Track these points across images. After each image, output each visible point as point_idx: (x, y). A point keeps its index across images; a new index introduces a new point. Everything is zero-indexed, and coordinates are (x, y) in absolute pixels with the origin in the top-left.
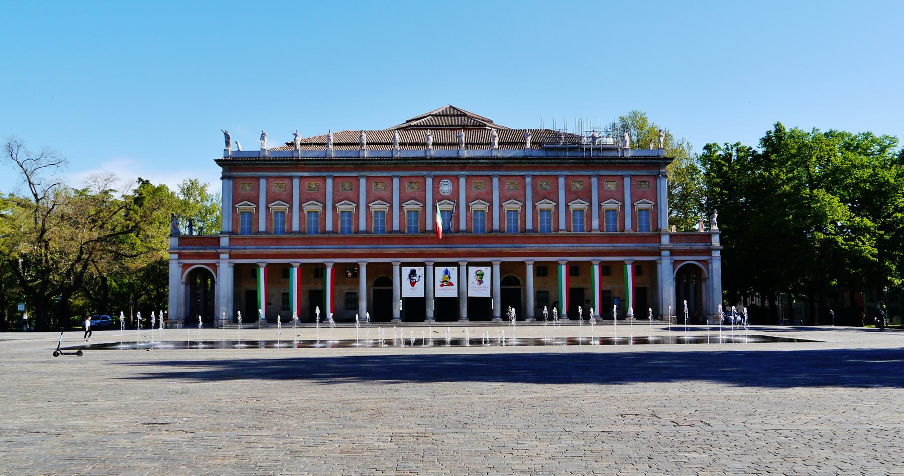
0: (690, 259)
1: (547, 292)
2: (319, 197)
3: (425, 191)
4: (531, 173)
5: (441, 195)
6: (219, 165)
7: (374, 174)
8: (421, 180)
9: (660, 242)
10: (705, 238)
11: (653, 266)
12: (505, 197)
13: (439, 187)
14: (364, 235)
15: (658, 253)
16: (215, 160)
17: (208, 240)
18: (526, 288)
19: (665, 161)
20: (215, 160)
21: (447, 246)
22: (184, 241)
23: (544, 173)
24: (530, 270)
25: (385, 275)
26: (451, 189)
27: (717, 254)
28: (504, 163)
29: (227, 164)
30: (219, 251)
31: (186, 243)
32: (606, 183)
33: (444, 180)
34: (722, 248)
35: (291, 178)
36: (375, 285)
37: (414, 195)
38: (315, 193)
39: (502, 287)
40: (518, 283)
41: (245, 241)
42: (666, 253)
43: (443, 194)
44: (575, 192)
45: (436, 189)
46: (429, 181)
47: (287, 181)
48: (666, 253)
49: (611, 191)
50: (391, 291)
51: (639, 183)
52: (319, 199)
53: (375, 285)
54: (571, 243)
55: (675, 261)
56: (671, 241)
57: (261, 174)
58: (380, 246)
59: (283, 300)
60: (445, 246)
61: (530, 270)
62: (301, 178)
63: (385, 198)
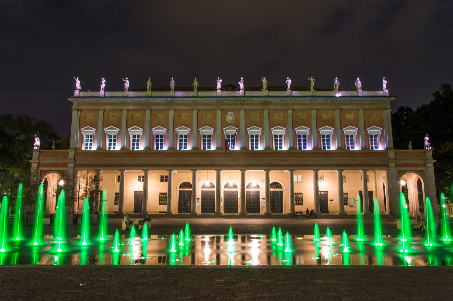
1: (302, 194)
3: (216, 120)
5: (227, 123)
7: (179, 108)
13: (226, 117)
14: (171, 150)
21: (232, 159)
22: (43, 154)
30: (67, 161)
31: (45, 155)
33: (230, 112)
35: (121, 110)
43: (228, 122)
46: (219, 112)
57: (100, 107)
58: (183, 159)
59: (115, 198)
60: (230, 159)
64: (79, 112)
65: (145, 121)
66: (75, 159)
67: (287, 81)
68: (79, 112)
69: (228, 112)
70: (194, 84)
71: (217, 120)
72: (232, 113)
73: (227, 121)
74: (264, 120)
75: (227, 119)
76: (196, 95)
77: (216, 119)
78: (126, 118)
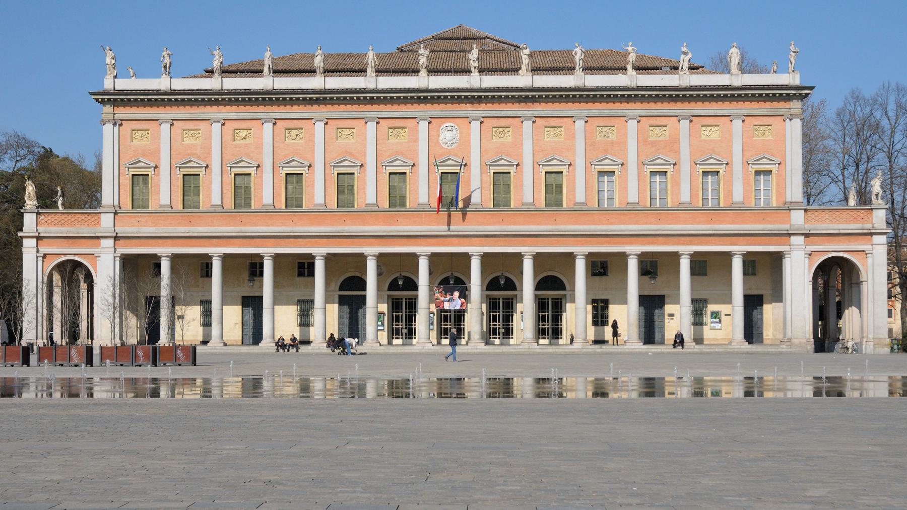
0: (836, 249)
3: (416, 140)
6: (97, 100)
9: (789, 221)
10: (862, 215)
11: (776, 259)
12: (543, 151)
13: (439, 136)
16: (92, 94)
17: (83, 217)
18: (574, 294)
19: (800, 92)
20: (92, 94)
22: (46, 219)
24: (580, 266)
25: (357, 274)
26: (458, 137)
28: (541, 96)
29: (109, 100)
32: (704, 128)
36: (341, 289)
38: (246, 145)
39: (540, 293)
40: (564, 289)
41: (139, 219)
43: (445, 146)
44: (653, 144)
45: (432, 140)
46: (423, 125)
47: (202, 125)
49: (711, 141)
50: (364, 298)
51: (756, 128)
52: (252, 155)
53: (341, 289)
54: (646, 223)
55: (812, 251)
56: (806, 220)
61: (580, 266)
64: (116, 128)
66: (115, 231)
67: (574, 52)
68: (116, 128)
69: (444, 122)
70: (368, 59)
71: (419, 142)
72: (452, 127)
73: (442, 144)
74: (524, 141)
75: (441, 138)
76: (372, 86)
77: (418, 138)
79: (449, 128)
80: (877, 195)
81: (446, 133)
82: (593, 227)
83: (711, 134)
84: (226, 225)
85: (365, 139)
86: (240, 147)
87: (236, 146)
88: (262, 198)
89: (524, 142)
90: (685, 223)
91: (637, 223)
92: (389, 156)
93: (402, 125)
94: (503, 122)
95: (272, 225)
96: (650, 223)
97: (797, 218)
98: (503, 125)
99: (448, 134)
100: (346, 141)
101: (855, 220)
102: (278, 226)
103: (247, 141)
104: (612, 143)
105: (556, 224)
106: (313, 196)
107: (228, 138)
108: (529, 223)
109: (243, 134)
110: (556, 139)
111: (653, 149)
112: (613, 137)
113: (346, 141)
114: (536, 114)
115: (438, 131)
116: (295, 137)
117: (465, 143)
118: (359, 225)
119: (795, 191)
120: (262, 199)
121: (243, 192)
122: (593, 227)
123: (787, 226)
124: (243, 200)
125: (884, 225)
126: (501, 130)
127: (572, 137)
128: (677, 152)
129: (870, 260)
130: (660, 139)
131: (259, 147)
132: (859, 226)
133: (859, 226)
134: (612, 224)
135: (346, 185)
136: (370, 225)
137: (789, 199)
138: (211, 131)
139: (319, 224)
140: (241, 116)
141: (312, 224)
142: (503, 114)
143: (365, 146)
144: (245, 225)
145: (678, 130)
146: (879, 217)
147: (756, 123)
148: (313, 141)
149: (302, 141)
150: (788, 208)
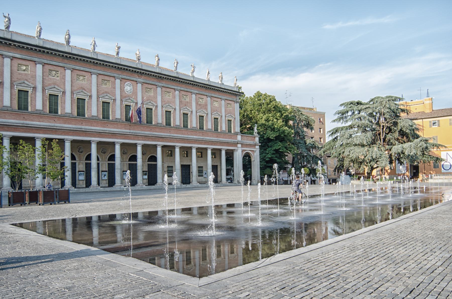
2: (30, 79)
3: (115, 88)
4: (179, 88)
8: (112, 79)
9: (237, 139)
15: (236, 144)
23: (186, 90)
27: (258, 147)
34: (260, 144)
37: (107, 90)
42: (239, 145)
43: (126, 92)
44: (200, 105)
46: (118, 81)
48: (239, 145)
52: (29, 80)
62: (12, 58)
63: (85, 88)
65: (36, 75)
75: (125, 89)
77: (115, 87)
78: (9, 67)
79: (129, 85)
80: (256, 133)
81: (128, 87)
82: (182, 136)
83: (216, 104)
84: (14, 119)
85: (91, 83)
86: (22, 75)
87: (19, 74)
88: (35, 105)
89: (158, 96)
90: (210, 137)
91: (196, 135)
92: (102, 94)
93: (108, 79)
94: (150, 86)
95: (43, 122)
96: (200, 136)
97: (239, 138)
98: (150, 87)
99: (128, 88)
100: (82, 82)
101: (252, 140)
102: (46, 122)
103: (26, 72)
104: (187, 102)
105: (170, 133)
106: (65, 108)
107: (15, 68)
108: (161, 132)
109: (24, 68)
110: (169, 97)
111: (200, 107)
112: (188, 100)
113: (81, 82)
114: (162, 85)
115: (124, 85)
116: (54, 75)
117: (135, 93)
118: (89, 126)
119: (238, 129)
120: (36, 106)
121: (23, 101)
122: (182, 136)
123: (236, 141)
124: (23, 106)
125: (258, 143)
126: (148, 89)
127: (174, 97)
128: (206, 109)
129: (255, 154)
130: (202, 103)
131: (34, 77)
132: (253, 142)
133: (253, 142)
134: (189, 135)
135: (81, 105)
136: (94, 126)
137: (236, 131)
138: (3, 62)
139: (69, 124)
140: (24, 57)
141: (65, 123)
142: (151, 82)
143: (91, 86)
144: (26, 120)
145: (207, 101)
146: (257, 139)
147: (228, 103)
148: (65, 79)
149: (59, 78)
150: (236, 134)
